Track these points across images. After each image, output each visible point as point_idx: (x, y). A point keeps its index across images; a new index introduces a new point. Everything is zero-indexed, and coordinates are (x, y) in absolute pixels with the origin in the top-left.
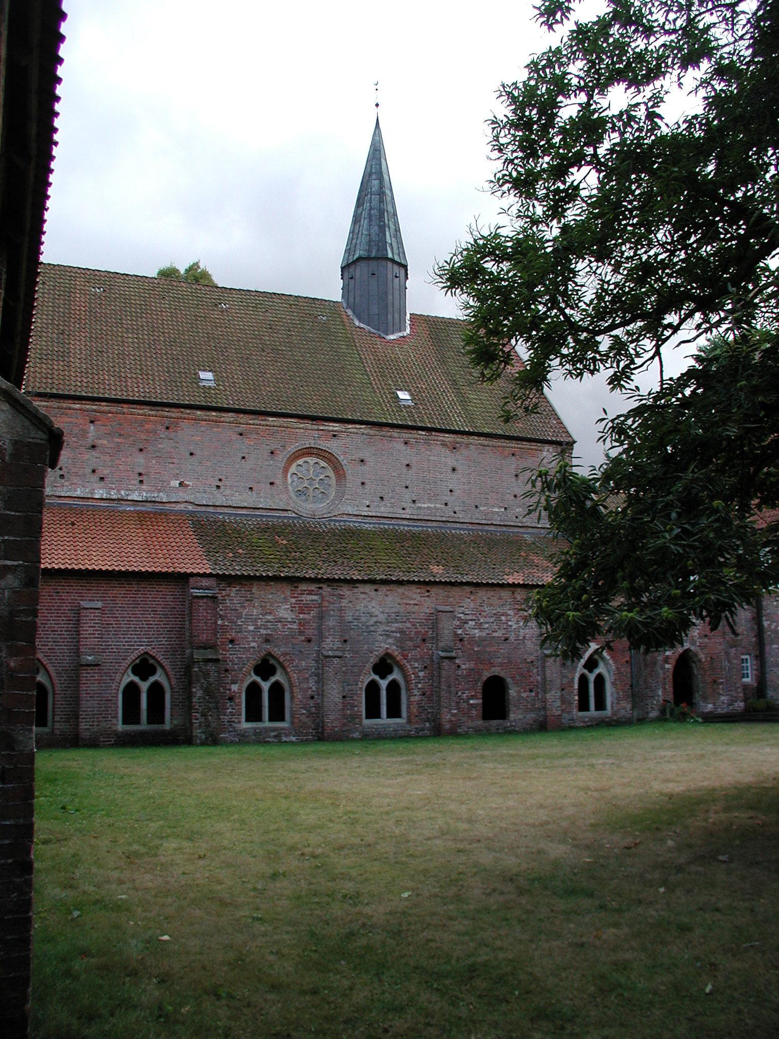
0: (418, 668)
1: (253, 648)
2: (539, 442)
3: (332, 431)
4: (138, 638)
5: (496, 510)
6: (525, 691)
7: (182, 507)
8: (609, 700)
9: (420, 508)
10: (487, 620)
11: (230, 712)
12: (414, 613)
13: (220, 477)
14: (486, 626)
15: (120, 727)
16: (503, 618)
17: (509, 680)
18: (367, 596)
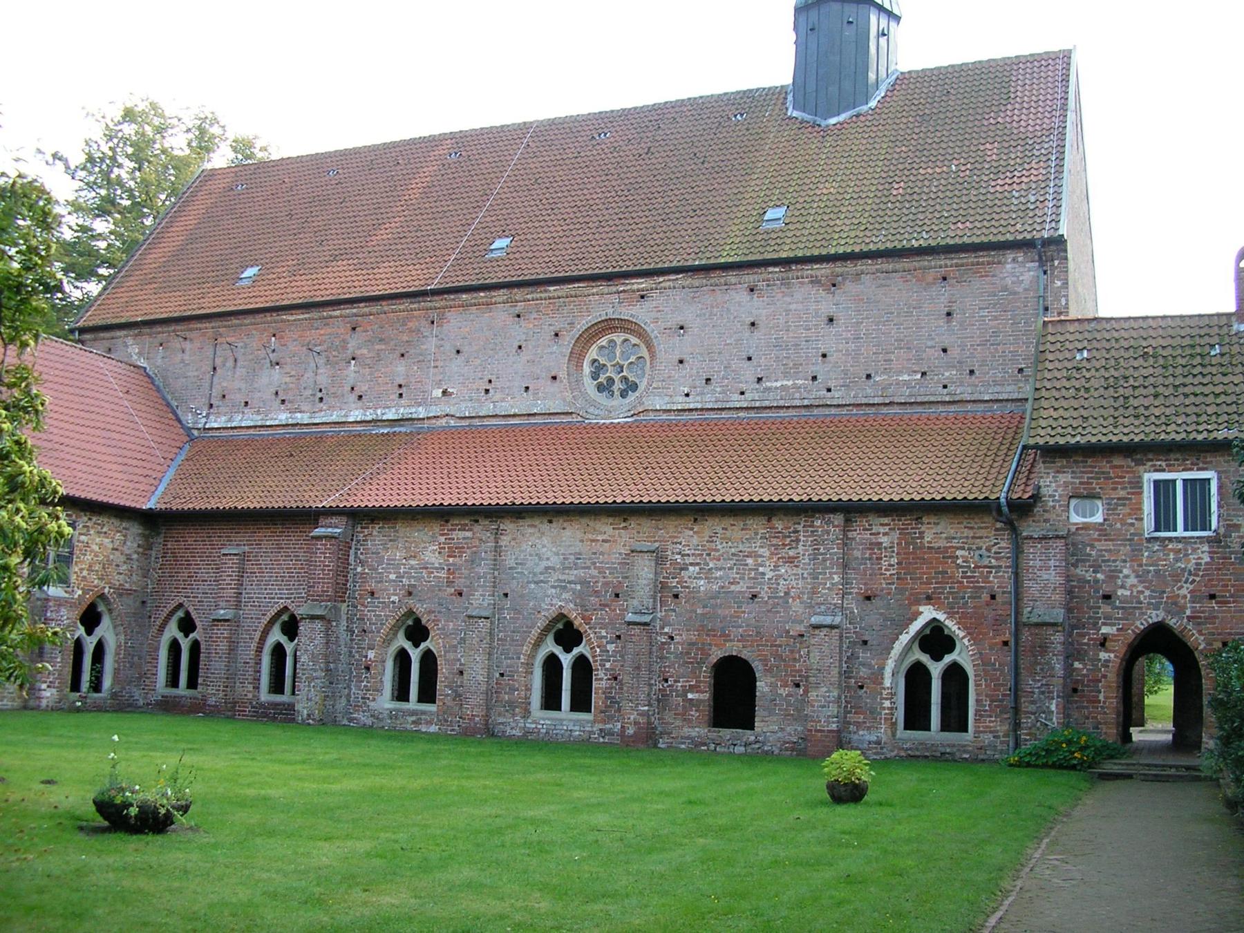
0: (606, 637)
1: (394, 602)
2: (994, 249)
3: (638, 290)
5: (906, 377)
6: (785, 685)
7: (443, 422)
8: (107, 682)
9: (768, 389)
10: (719, 564)
11: (365, 686)
12: (602, 554)
14: (719, 573)
15: (265, 696)
16: (750, 561)
17: (757, 666)
18: (537, 530)
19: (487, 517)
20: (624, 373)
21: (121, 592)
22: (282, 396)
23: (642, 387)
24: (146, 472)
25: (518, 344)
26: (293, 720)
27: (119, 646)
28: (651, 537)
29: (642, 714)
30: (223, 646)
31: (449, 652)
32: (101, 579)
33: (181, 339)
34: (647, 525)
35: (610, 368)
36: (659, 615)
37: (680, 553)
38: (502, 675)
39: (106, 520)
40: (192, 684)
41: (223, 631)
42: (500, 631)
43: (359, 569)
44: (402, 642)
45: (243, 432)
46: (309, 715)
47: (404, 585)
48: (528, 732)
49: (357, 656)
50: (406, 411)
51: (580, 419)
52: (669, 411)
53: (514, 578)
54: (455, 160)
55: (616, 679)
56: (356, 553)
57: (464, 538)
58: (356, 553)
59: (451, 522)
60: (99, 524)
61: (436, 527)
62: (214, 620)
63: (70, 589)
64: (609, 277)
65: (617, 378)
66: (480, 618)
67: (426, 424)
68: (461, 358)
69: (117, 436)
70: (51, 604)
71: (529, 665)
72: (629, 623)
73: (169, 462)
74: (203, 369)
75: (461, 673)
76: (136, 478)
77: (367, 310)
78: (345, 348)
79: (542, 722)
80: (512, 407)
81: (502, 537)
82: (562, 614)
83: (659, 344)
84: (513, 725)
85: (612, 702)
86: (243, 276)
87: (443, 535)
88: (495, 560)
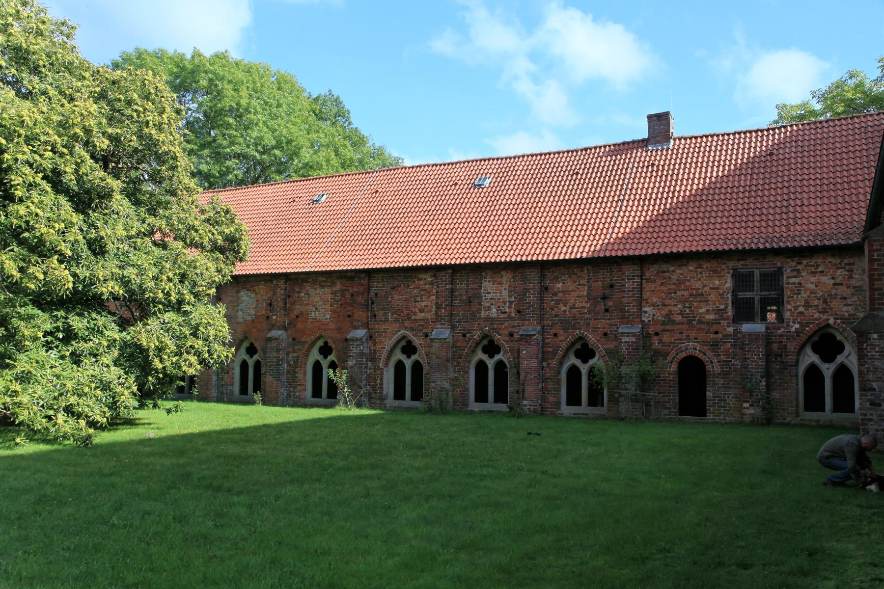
32: (824, 312)
39: (820, 261)
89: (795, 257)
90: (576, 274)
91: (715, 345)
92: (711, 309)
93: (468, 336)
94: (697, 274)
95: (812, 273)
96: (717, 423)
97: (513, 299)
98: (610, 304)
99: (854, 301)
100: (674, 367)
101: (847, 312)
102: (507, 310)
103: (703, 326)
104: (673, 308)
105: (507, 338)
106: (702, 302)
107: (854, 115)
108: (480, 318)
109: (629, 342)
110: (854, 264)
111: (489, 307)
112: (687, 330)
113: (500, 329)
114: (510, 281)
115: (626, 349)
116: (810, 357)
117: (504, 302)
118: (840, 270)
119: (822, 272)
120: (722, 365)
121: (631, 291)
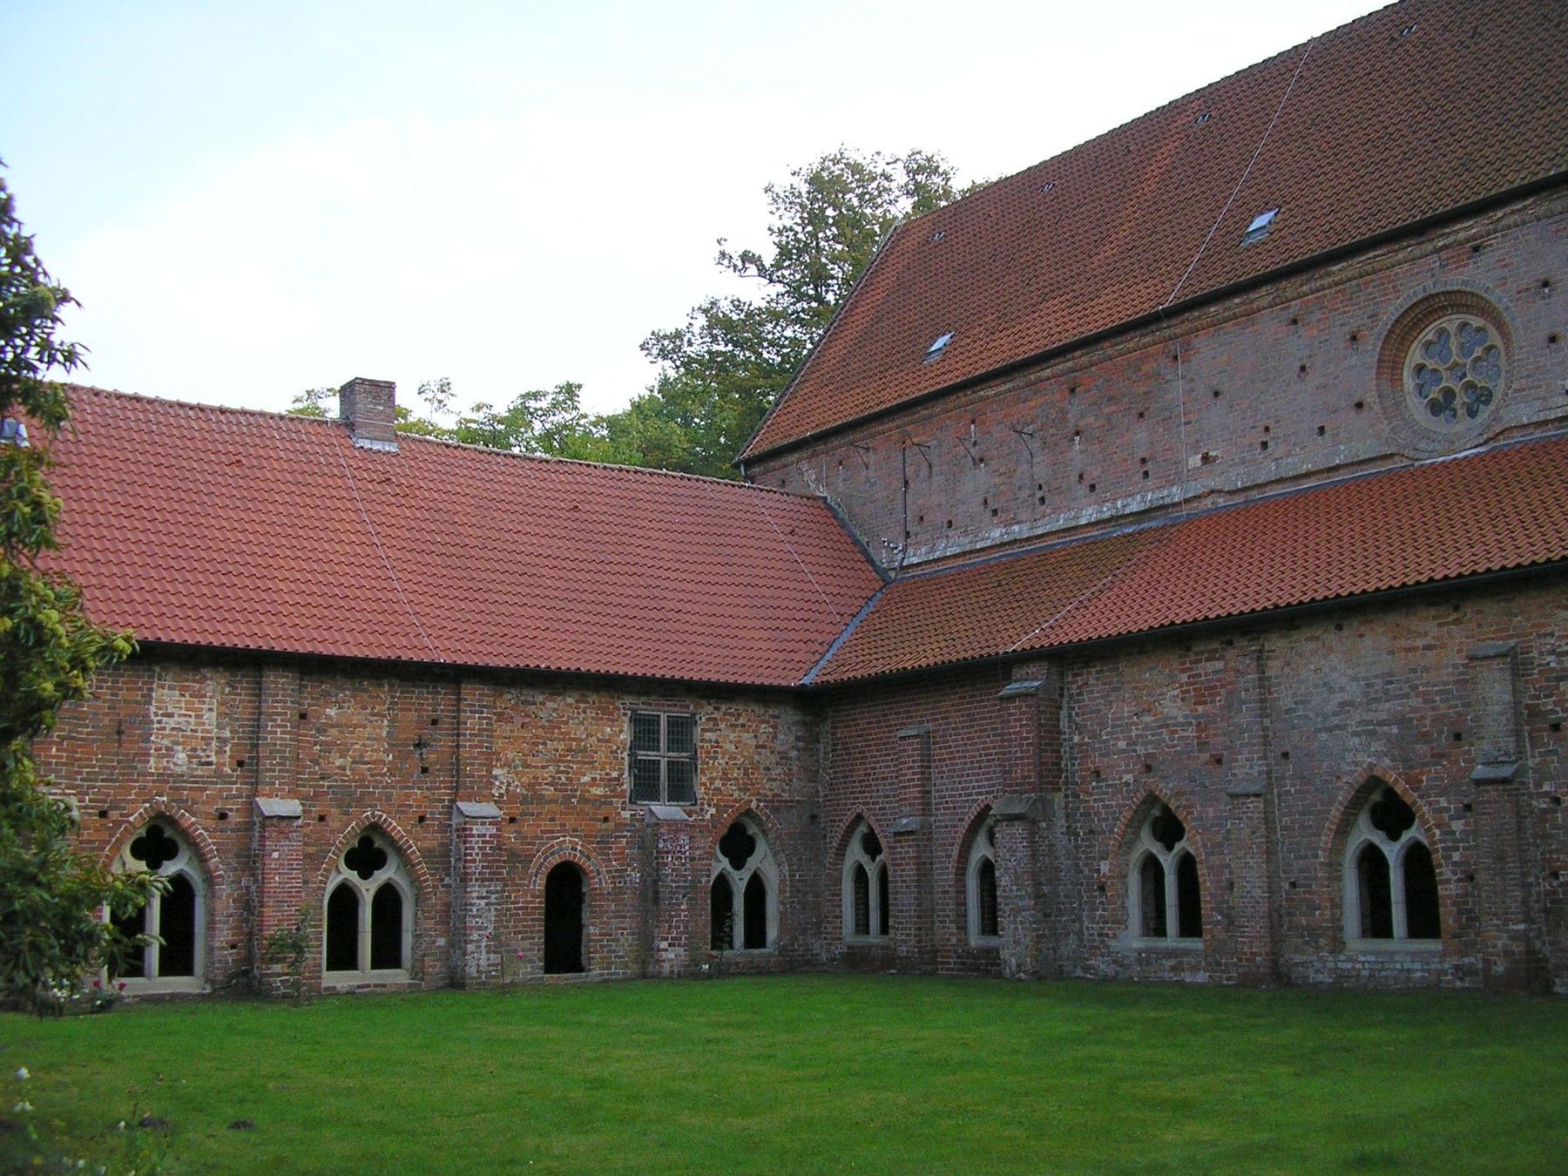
0: (1447, 810)
1: (1127, 784)
3: (1468, 240)
4: (977, 781)
7: (1207, 503)
11: (1101, 916)
12: (1426, 669)
13: (1266, 422)
15: (975, 940)
18: (1320, 644)
19: (1244, 634)
20: (1469, 378)
21: (777, 805)
22: (992, 505)
23: (1498, 393)
24: (808, 636)
25: (1299, 364)
26: (999, 975)
27: (783, 881)
28: (1502, 630)
29: (1514, 937)
30: (910, 870)
31: (1212, 854)
32: (745, 790)
33: (862, 452)
34: (1492, 610)
35: (1445, 374)
36: (1530, 763)
37: (1553, 652)
38: (1293, 885)
39: (741, 708)
40: (885, 929)
41: (907, 849)
42: (1283, 815)
43: (1076, 739)
44: (1148, 843)
45: (951, 564)
46: (1018, 966)
47: (1139, 756)
48: (1341, 976)
49: (1086, 871)
50: (1155, 496)
51: (1406, 462)
52: (1545, 423)
53: (1294, 727)
54: (1203, 125)
55: (1471, 878)
56: (1070, 715)
57: (1215, 672)
58: (1070, 715)
59: (1194, 649)
60: (732, 715)
61: (1173, 661)
62: (896, 834)
63: (697, 808)
64: (1419, 230)
65: (1457, 387)
66: (1248, 796)
67: (1185, 511)
68: (1222, 402)
69: (768, 593)
70: (662, 830)
71: (1334, 867)
72: (1479, 782)
73: (847, 619)
74: (892, 487)
75: (1231, 885)
76: (789, 646)
77: (1085, 359)
78: (1064, 420)
79: (1363, 959)
80: (1303, 463)
81: (1270, 663)
82: (1374, 777)
83: (1513, 319)
84: (1318, 965)
85: (1470, 918)
86: (933, 349)
87: (1184, 671)
88: (1261, 701)
89: (712, 698)
90: (365, 691)
91: (603, 843)
92: (598, 777)
93: (114, 815)
94: (579, 713)
95: (731, 725)
96: (606, 981)
97: (227, 734)
98: (433, 757)
99: (779, 775)
100: (540, 884)
101: (772, 790)
102: (213, 759)
103: (587, 807)
104: (539, 773)
105: (212, 824)
106: (585, 763)
107: (623, 466)
108: (144, 774)
109: (484, 835)
110: (778, 717)
111: (167, 748)
112: (561, 813)
113: (195, 802)
114: (223, 693)
115: (480, 848)
116: (719, 861)
117: (207, 740)
118: (764, 726)
119: (743, 725)
120: (613, 877)
121: (475, 735)
